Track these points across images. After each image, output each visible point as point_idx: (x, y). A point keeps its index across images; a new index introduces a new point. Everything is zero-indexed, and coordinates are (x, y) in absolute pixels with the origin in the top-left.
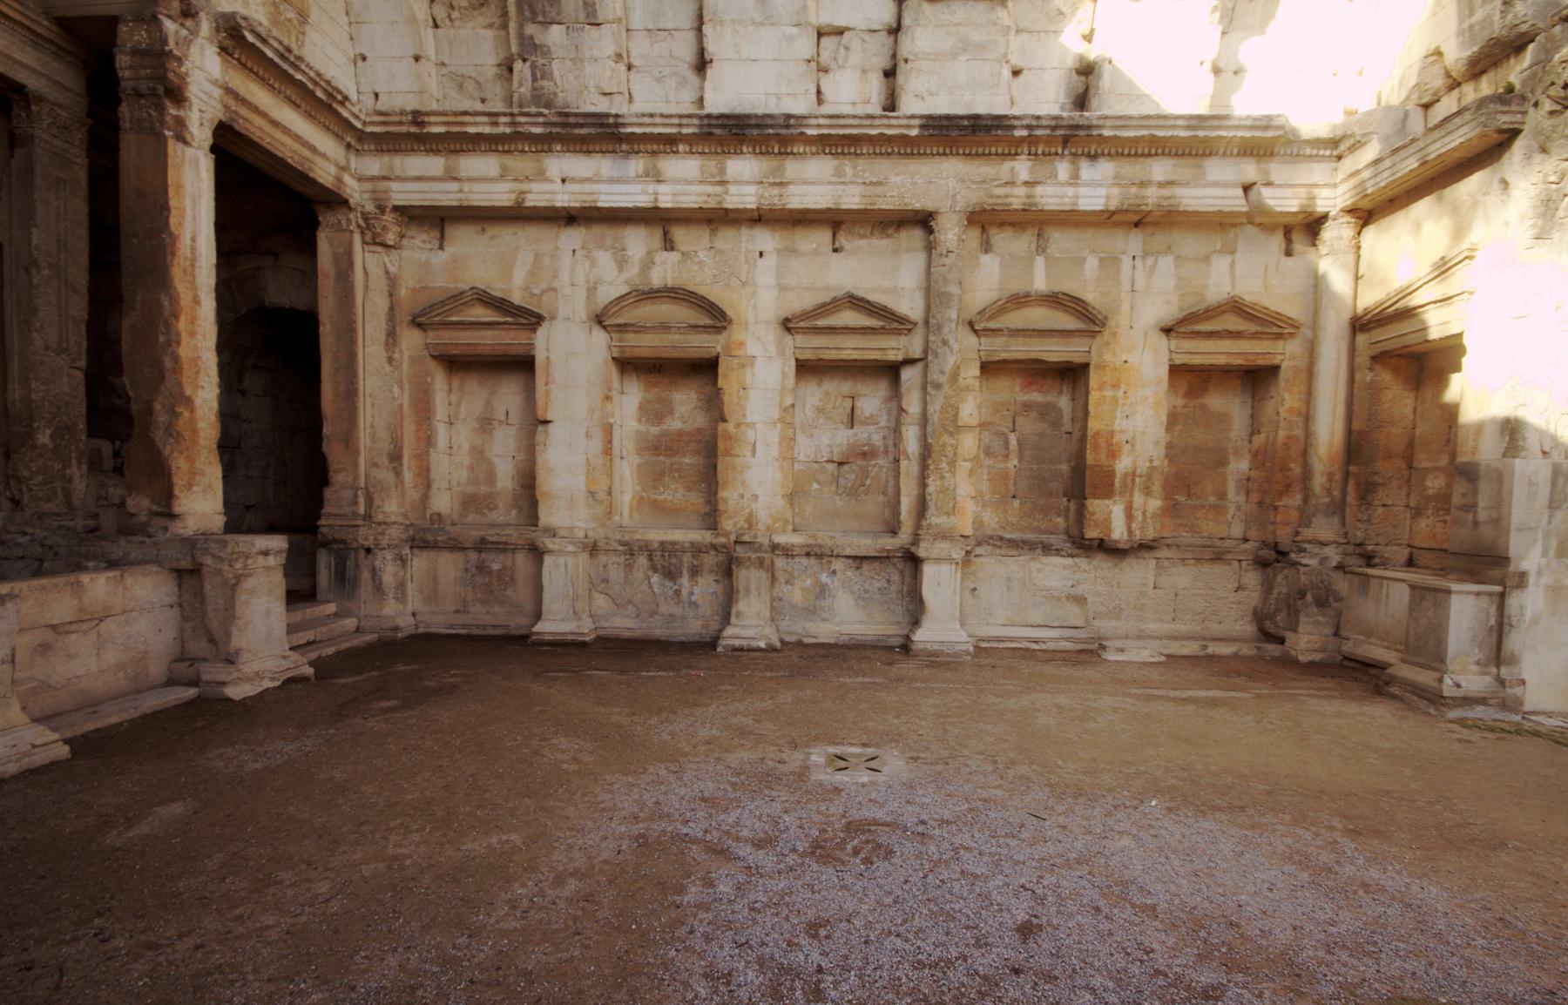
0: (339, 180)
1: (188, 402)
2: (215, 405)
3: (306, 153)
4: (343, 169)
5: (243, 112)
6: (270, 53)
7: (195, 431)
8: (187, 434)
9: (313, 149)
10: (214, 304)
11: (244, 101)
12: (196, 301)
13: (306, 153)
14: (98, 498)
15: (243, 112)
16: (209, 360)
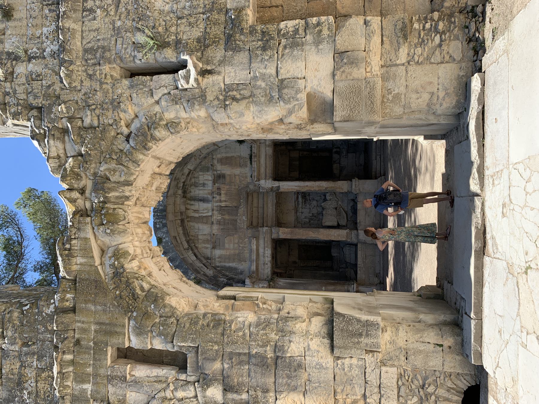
0: (269, 146)
1: (326, 188)
2: (326, 182)
3: (268, 157)
4: (266, 145)
5: (268, 175)
6: (256, 174)
7: (332, 187)
8: (333, 189)
9: (266, 155)
10: (306, 182)
11: (266, 175)
12: (307, 186)
13: (268, 157)
14: (346, 157)
15: (268, 175)
16: (318, 183)
